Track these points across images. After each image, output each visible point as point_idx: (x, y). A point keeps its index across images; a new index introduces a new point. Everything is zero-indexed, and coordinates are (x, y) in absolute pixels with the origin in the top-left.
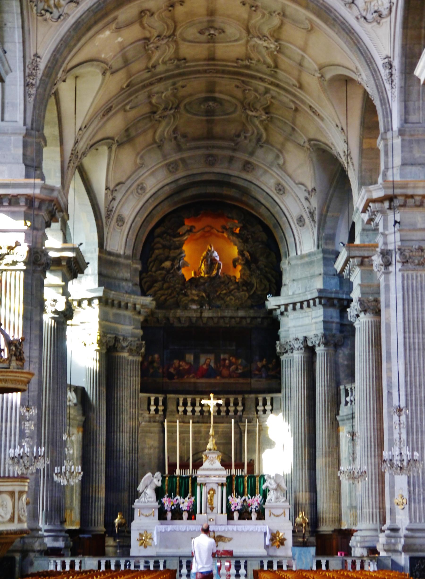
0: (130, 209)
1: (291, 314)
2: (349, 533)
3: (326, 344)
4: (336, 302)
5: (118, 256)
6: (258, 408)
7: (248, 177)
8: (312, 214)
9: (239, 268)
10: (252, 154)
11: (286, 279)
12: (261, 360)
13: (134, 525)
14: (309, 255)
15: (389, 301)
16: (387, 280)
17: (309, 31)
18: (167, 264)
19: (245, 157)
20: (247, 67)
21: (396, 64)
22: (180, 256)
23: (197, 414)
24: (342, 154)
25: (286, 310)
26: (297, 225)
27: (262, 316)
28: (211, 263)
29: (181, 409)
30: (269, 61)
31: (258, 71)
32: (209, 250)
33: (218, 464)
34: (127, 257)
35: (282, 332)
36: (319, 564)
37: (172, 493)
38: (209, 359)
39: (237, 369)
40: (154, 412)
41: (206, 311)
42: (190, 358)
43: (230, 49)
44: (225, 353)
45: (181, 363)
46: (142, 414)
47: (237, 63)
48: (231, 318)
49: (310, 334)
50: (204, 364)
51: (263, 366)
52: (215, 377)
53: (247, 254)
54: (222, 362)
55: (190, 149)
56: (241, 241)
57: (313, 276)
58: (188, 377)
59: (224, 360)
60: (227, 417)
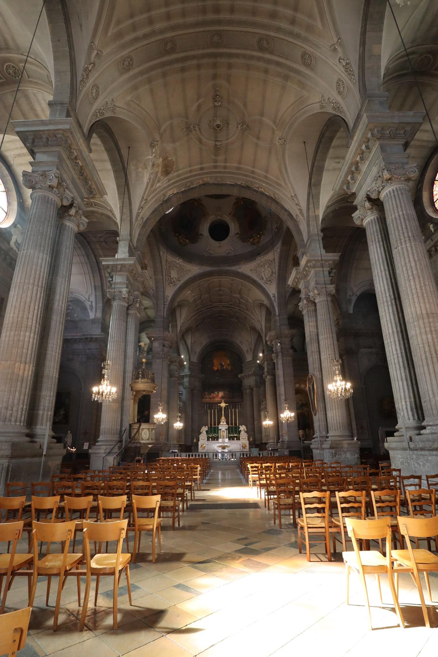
0: (198, 349)
2: (266, 444)
3: (256, 387)
8: (251, 349)
11: (244, 369)
13: (199, 443)
16: (277, 361)
20: (231, 305)
21: (276, 296)
28: (222, 366)
30: (238, 302)
33: (225, 423)
35: (243, 384)
36: (260, 454)
37: (211, 432)
49: (252, 385)
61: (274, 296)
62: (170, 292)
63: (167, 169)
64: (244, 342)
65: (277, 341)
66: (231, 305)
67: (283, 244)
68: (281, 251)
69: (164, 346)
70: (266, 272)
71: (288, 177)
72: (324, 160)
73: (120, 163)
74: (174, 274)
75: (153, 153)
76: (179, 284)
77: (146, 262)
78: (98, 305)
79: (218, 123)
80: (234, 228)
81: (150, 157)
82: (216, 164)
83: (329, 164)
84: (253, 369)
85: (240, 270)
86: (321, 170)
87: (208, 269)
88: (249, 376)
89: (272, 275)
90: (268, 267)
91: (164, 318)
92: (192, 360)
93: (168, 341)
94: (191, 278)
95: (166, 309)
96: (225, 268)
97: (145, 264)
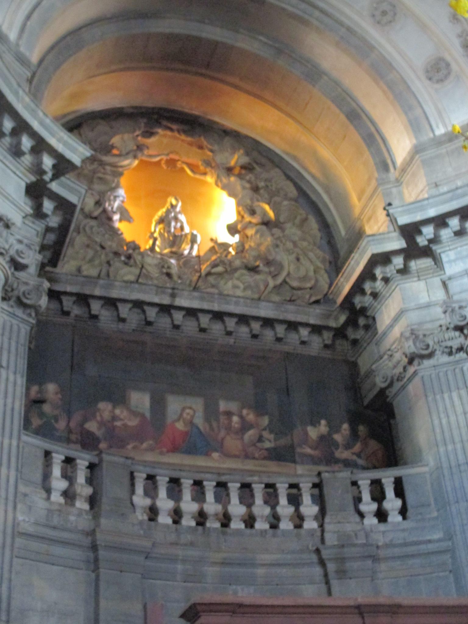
6: (363, 508)
12: (314, 423)
23: (188, 522)
25: (435, 240)
26: (427, 82)
27: (312, 321)
29: (141, 500)
32: (172, 206)
38: (190, 408)
39: (260, 439)
40: (62, 500)
41: (186, 293)
42: (140, 400)
44: (228, 398)
45: (117, 412)
46: (25, 495)
50: (178, 420)
51: (322, 438)
52: (207, 454)
54: (222, 418)
56: (248, 185)
58: (134, 448)
59: (229, 414)
60: (274, 536)
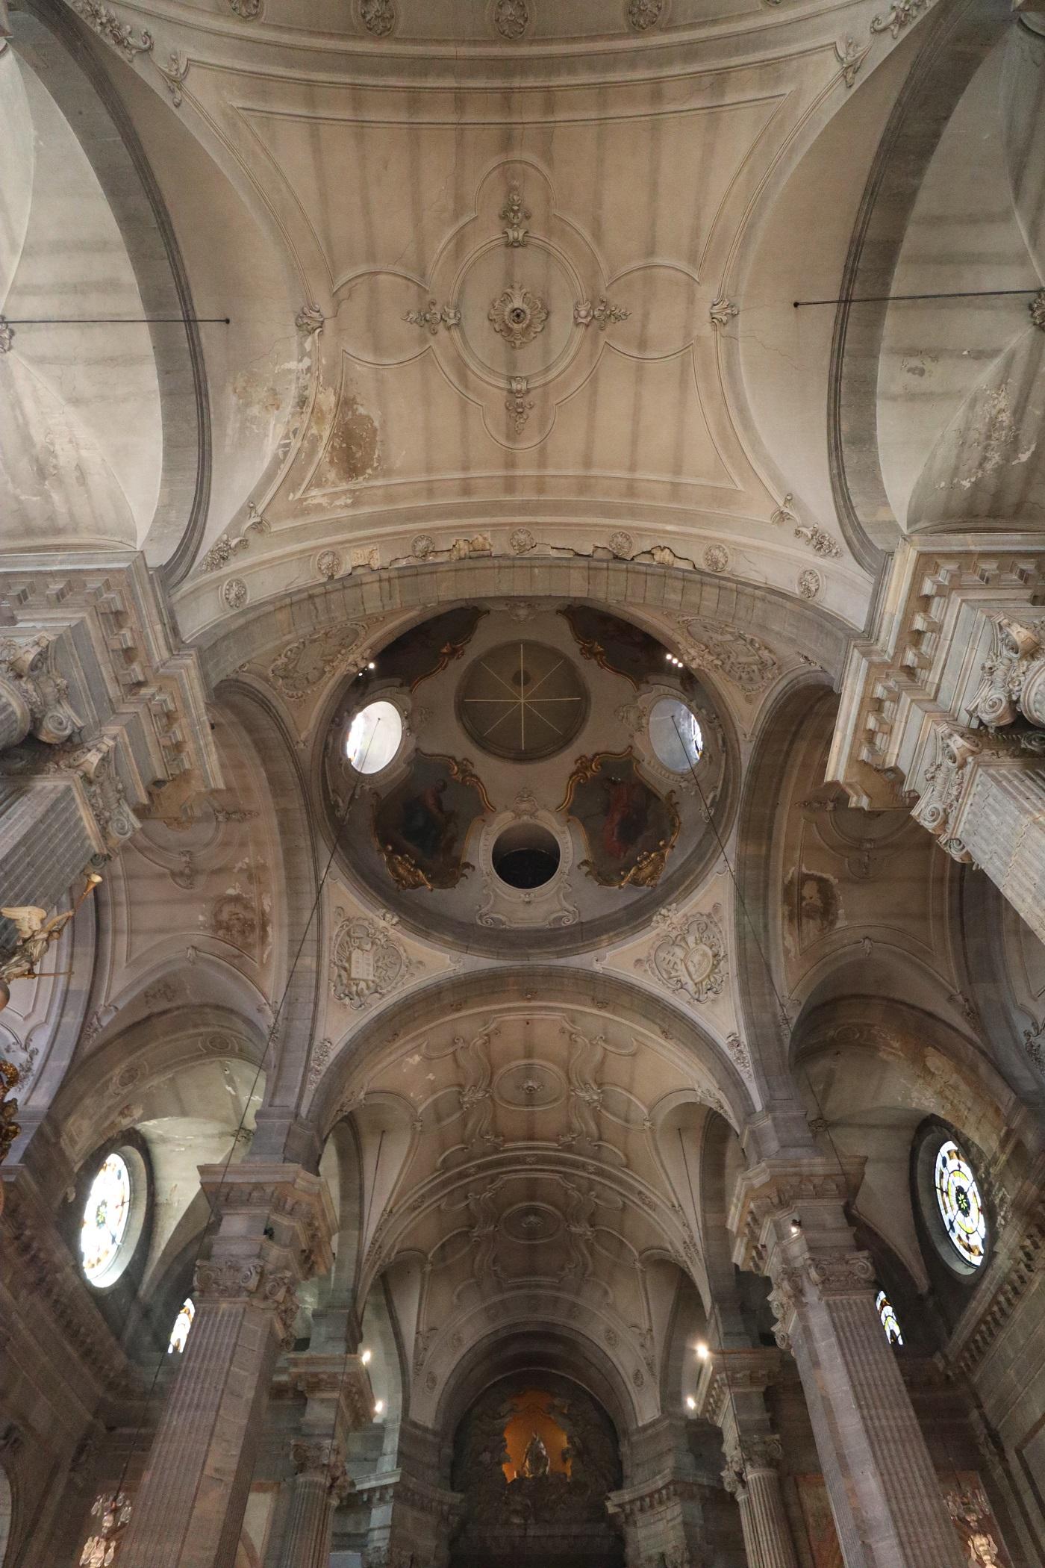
0: (445, 1366)
1: (640, 1519)
4: (695, 1489)
5: (426, 1429)
7: (575, 1325)
9: (569, 1464)
10: (578, 1293)
11: (627, 1469)
14: (652, 1424)
15: (816, 1356)
17: (634, 1055)
18: (486, 1457)
19: (571, 1297)
20: (569, 1148)
21: (744, 1039)
22: (501, 1445)
24: (680, 1248)
25: (632, 1512)
28: (537, 1459)
31: (580, 1155)
34: (435, 1433)
35: (630, 1551)
43: (549, 1117)
47: (557, 1141)
48: (563, 1537)
49: (669, 1549)
53: (576, 1440)
55: (513, 1288)
57: (661, 1455)
61: (736, 1043)
62: (338, 1028)
63: (353, 450)
64: (621, 1327)
65: (780, 1215)
66: (569, 1148)
67: (745, 835)
68: (741, 863)
69: (269, 1233)
70: (693, 961)
71: (756, 443)
72: (872, 355)
73: (189, 364)
74: (363, 966)
75: (303, 354)
76: (378, 1006)
77: (267, 904)
78: (52, 1064)
79: (517, 303)
80: (572, 847)
81: (293, 365)
82: (510, 473)
83: (890, 374)
84: (669, 1462)
85: (597, 967)
86: (866, 389)
87: (481, 962)
88: (650, 1502)
89: (715, 966)
90: (699, 941)
91: (297, 1115)
92: (414, 1415)
93: (291, 1212)
94: (424, 990)
95: (311, 1088)
96: (545, 962)
97: (263, 913)
